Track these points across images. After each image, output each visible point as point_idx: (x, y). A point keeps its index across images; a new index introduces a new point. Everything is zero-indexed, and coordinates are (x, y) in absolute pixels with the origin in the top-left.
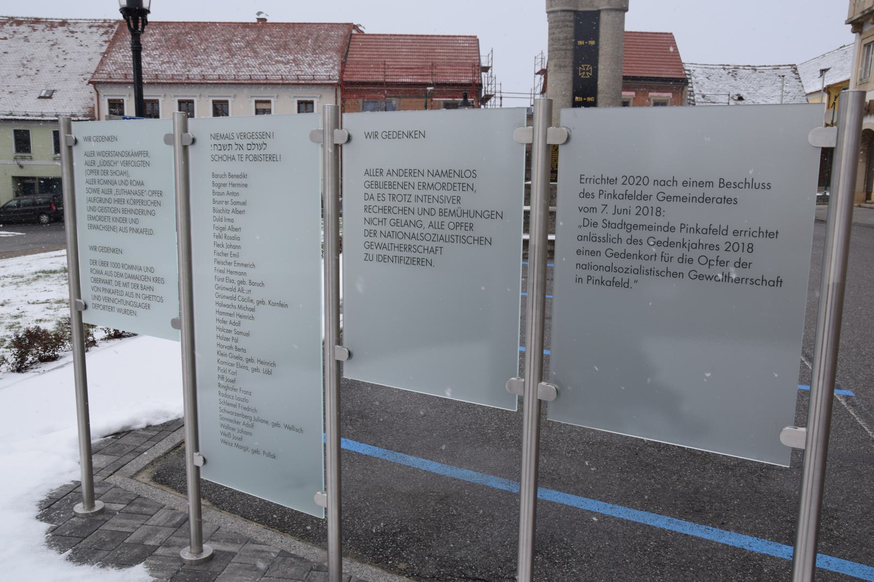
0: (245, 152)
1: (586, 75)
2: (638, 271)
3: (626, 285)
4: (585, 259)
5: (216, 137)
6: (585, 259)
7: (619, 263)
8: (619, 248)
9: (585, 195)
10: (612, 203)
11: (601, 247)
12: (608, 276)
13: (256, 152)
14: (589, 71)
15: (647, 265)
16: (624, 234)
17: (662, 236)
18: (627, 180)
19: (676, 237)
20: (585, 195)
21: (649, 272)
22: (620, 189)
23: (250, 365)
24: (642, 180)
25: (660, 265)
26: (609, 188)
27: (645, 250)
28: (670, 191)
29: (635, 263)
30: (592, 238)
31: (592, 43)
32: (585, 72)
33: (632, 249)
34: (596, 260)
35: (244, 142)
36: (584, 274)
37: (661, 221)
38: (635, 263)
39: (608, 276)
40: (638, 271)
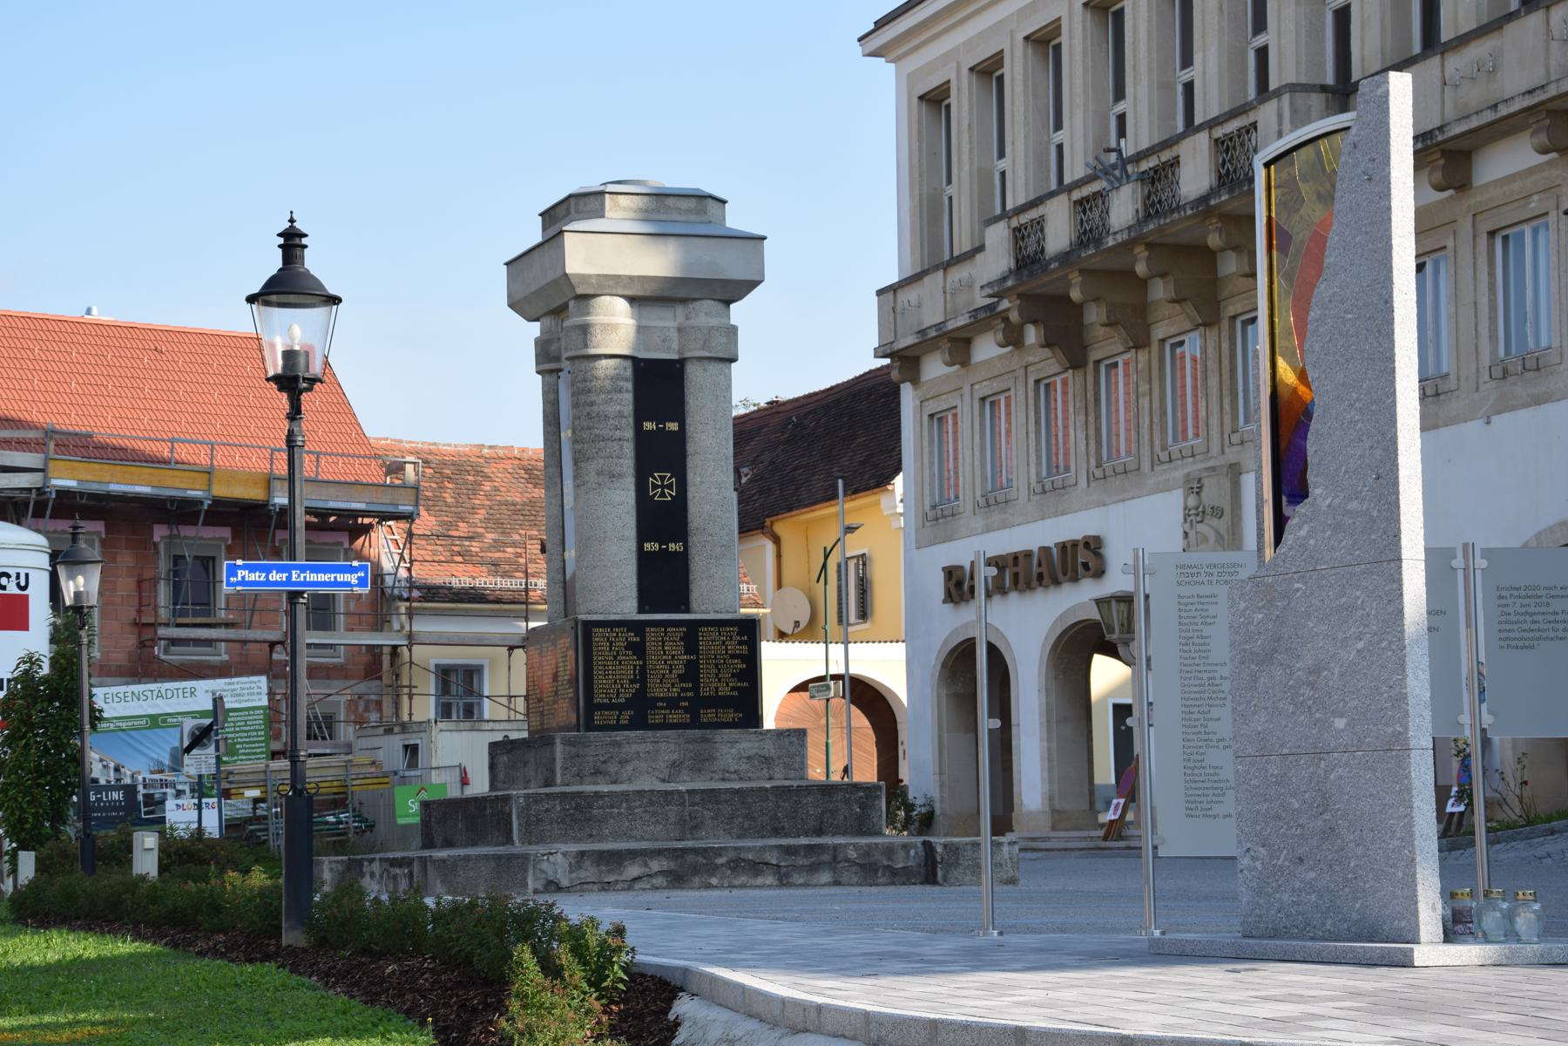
0: (1215, 578)
1: (663, 495)
2: (1539, 639)
3: (1533, 647)
4: (1505, 635)
5: (1182, 567)
6: (1505, 635)
7: (1526, 635)
8: (1525, 627)
9: (1501, 597)
10: (1518, 601)
11: (1515, 627)
12: (1520, 644)
13: (1227, 578)
14: (670, 487)
15: (1544, 635)
16: (1528, 619)
17: (1551, 618)
18: (1527, 588)
19: (1559, 618)
20: (1501, 597)
21: (1546, 638)
22: (1523, 593)
23: (1221, 744)
24: (1537, 587)
25: (1552, 634)
26: (1516, 593)
27: (1542, 626)
28: (1553, 593)
29: (1537, 635)
30: (1507, 622)
31: (673, 426)
32: (662, 486)
33: (1534, 627)
34: (1511, 635)
35: (1215, 571)
36: (1505, 644)
37: (1550, 610)
38: (1537, 635)
39: (1520, 644)
40: (1539, 639)
